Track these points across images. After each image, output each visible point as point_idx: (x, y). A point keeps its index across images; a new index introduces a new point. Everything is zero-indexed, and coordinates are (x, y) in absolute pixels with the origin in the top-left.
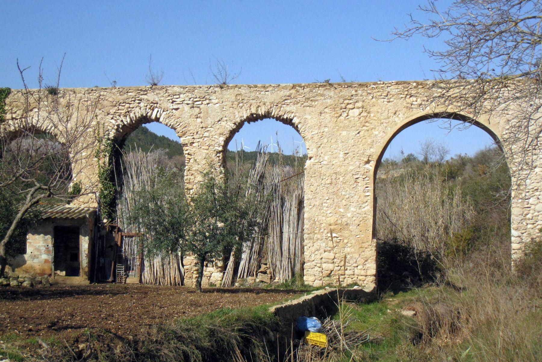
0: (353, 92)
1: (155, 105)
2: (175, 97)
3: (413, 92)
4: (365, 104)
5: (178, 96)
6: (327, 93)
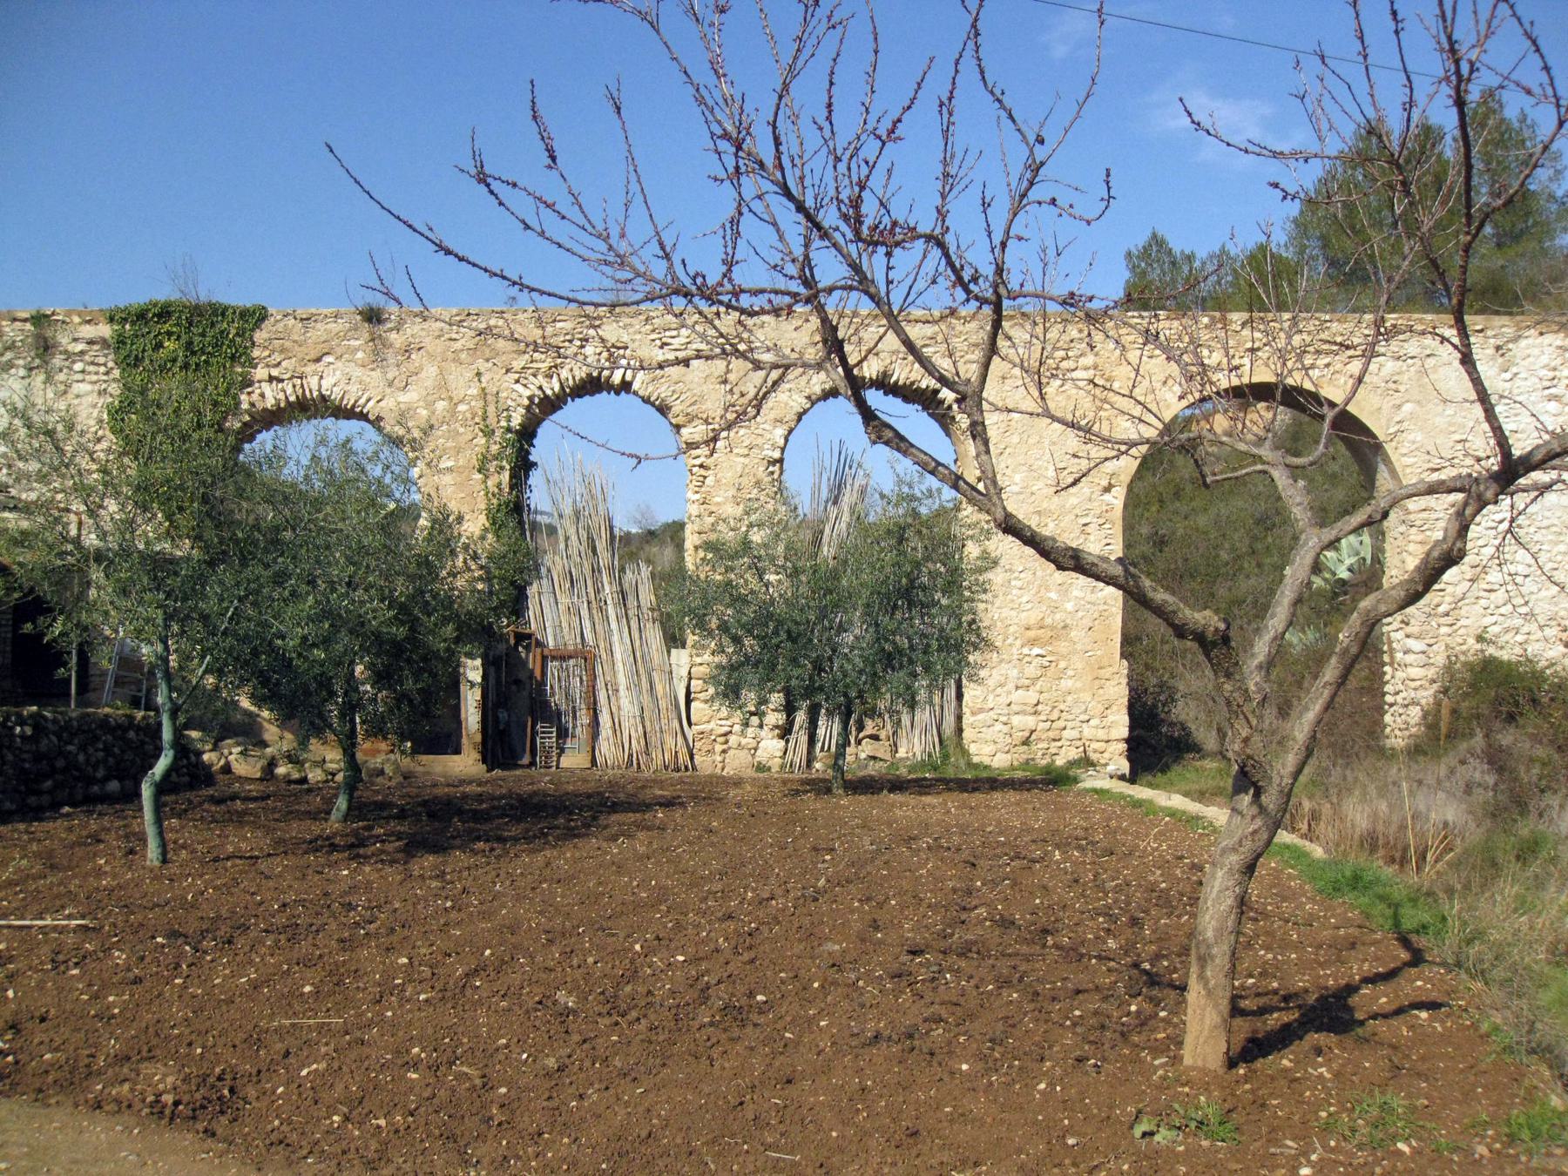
1: (621, 352)
2: (668, 334)
4: (1099, 361)
5: (674, 333)
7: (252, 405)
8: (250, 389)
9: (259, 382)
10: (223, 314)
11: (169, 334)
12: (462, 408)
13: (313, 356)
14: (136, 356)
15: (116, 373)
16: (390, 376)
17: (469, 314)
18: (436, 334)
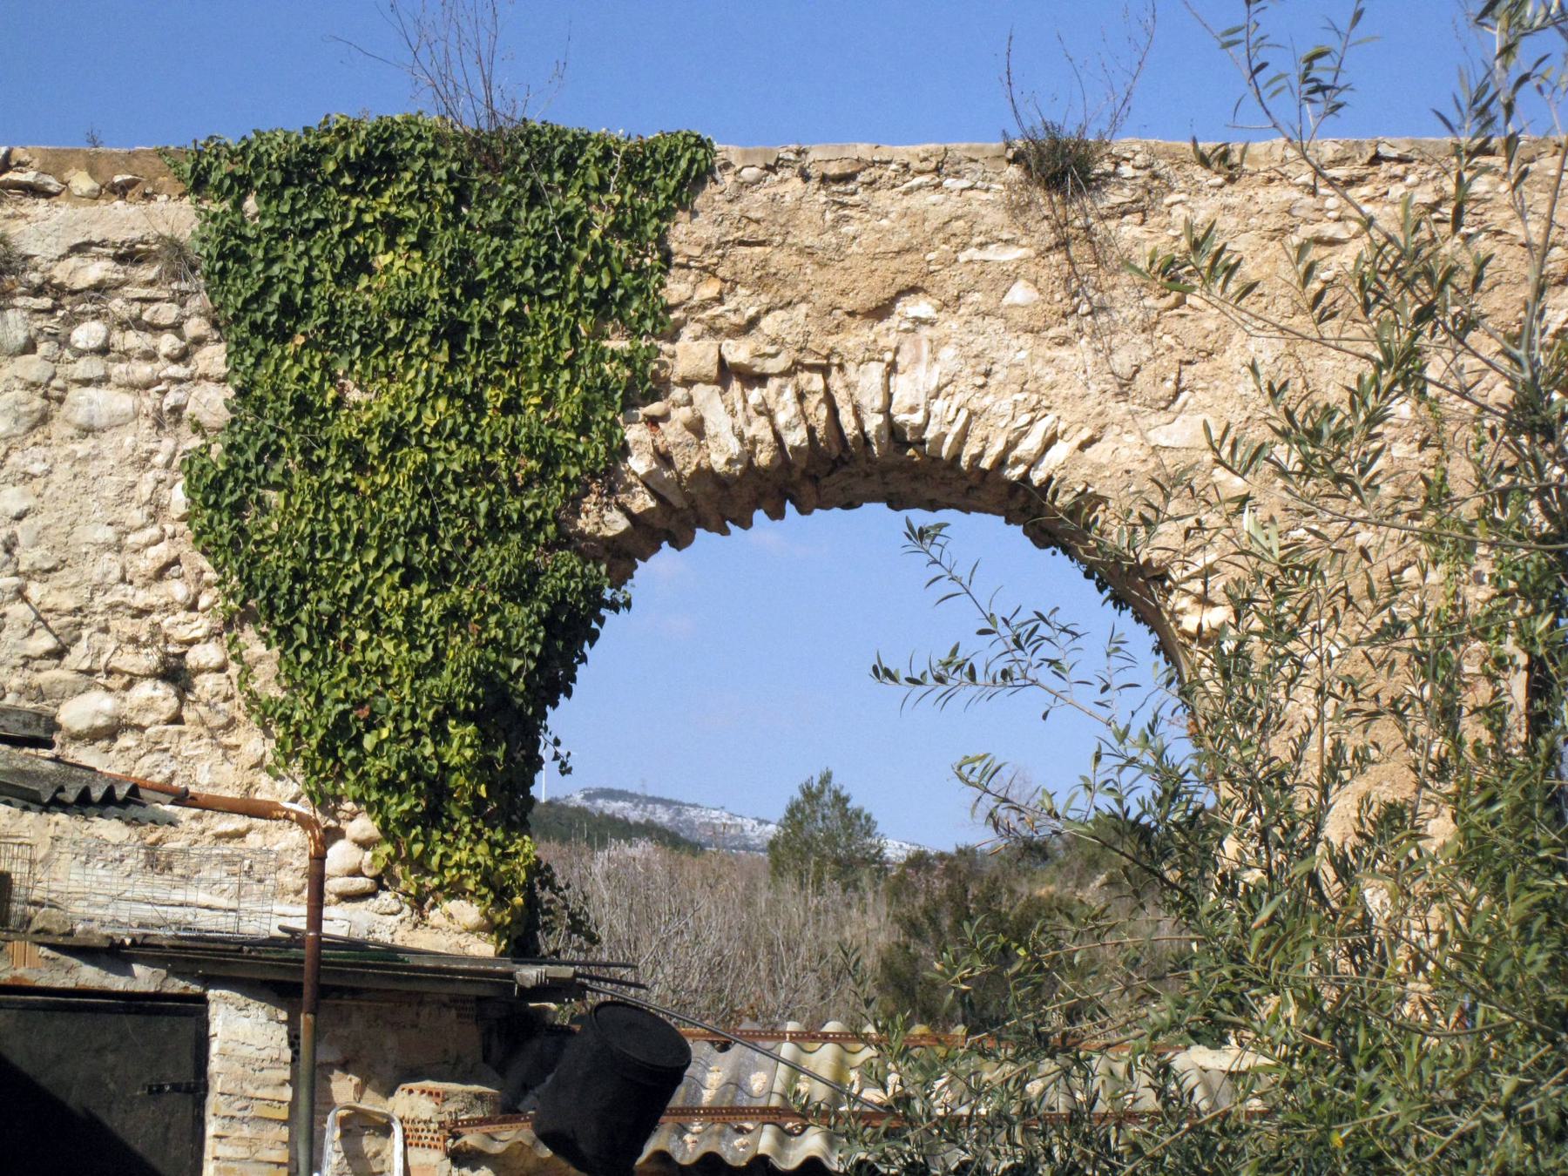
7: (664, 458)
8: (655, 408)
9: (688, 382)
10: (568, 164)
11: (393, 227)
13: (865, 297)
14: (286, 299)
15: (213, 358)
16: (1123, 361)
17: (1376, 159)
18: (1273, 222)
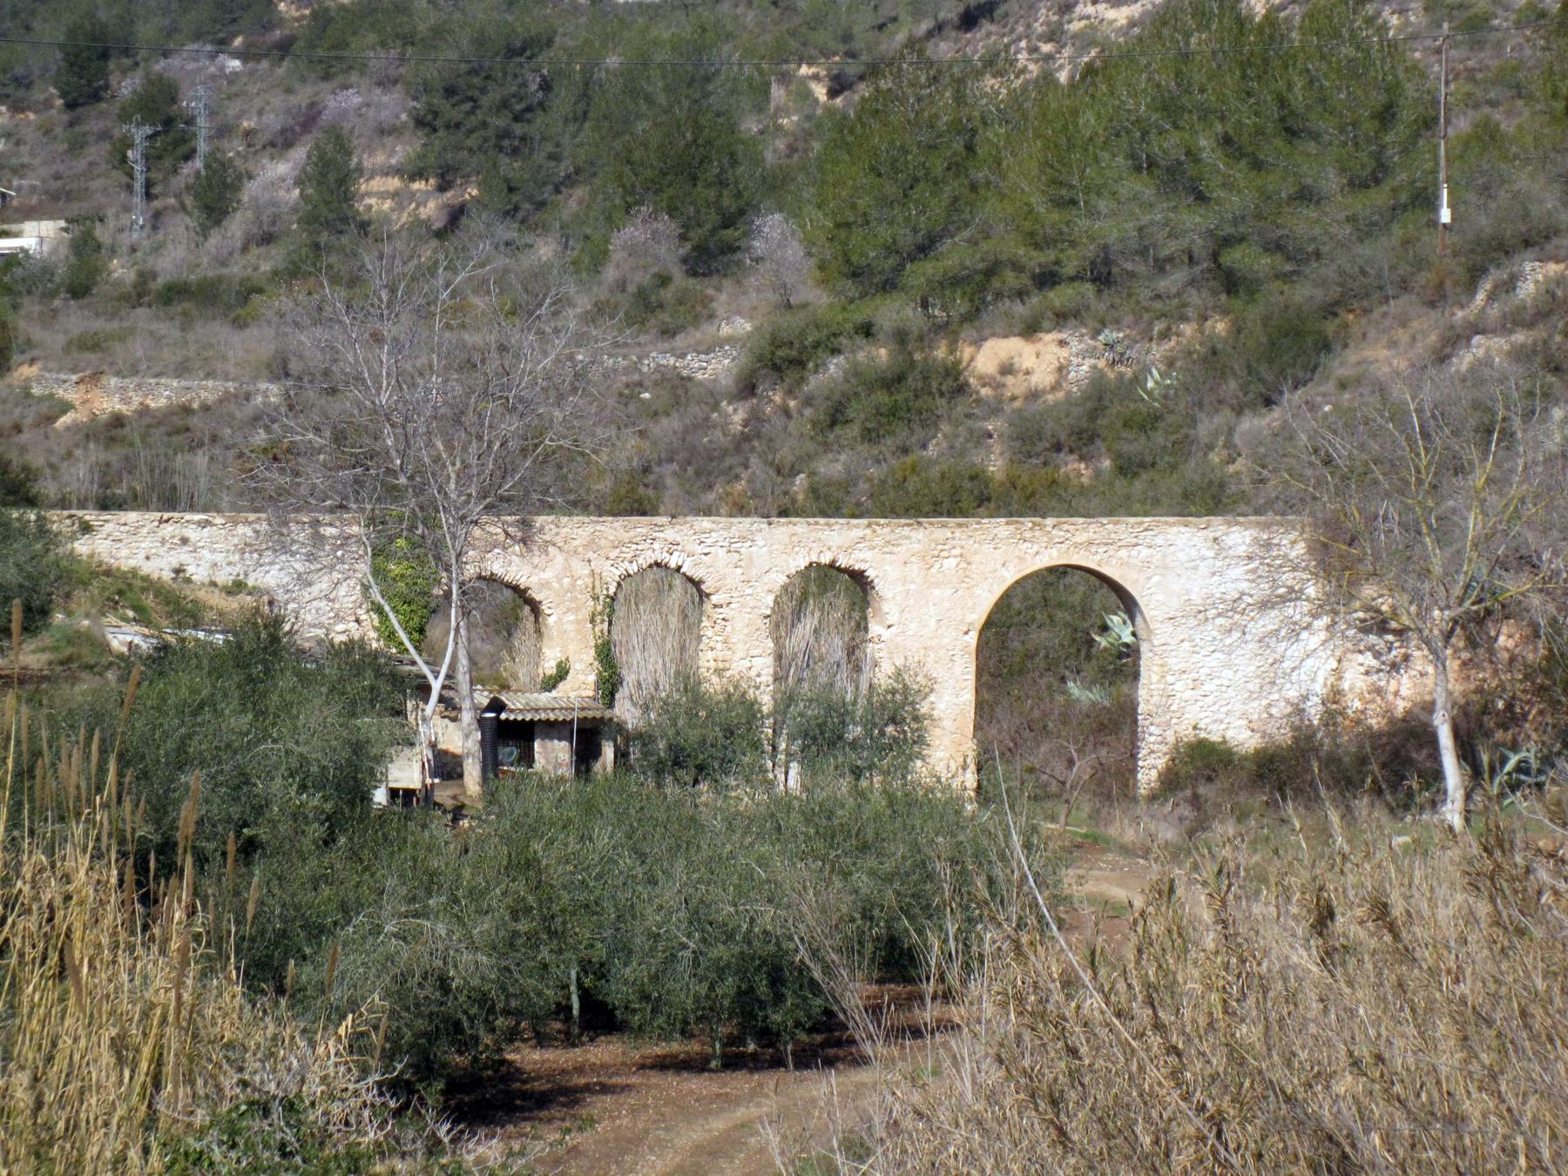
0: (949, 535)
3: (1028, 535)
6: (914, 535)
12: (579, 582)
